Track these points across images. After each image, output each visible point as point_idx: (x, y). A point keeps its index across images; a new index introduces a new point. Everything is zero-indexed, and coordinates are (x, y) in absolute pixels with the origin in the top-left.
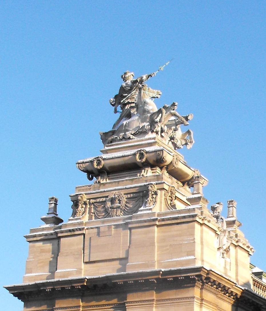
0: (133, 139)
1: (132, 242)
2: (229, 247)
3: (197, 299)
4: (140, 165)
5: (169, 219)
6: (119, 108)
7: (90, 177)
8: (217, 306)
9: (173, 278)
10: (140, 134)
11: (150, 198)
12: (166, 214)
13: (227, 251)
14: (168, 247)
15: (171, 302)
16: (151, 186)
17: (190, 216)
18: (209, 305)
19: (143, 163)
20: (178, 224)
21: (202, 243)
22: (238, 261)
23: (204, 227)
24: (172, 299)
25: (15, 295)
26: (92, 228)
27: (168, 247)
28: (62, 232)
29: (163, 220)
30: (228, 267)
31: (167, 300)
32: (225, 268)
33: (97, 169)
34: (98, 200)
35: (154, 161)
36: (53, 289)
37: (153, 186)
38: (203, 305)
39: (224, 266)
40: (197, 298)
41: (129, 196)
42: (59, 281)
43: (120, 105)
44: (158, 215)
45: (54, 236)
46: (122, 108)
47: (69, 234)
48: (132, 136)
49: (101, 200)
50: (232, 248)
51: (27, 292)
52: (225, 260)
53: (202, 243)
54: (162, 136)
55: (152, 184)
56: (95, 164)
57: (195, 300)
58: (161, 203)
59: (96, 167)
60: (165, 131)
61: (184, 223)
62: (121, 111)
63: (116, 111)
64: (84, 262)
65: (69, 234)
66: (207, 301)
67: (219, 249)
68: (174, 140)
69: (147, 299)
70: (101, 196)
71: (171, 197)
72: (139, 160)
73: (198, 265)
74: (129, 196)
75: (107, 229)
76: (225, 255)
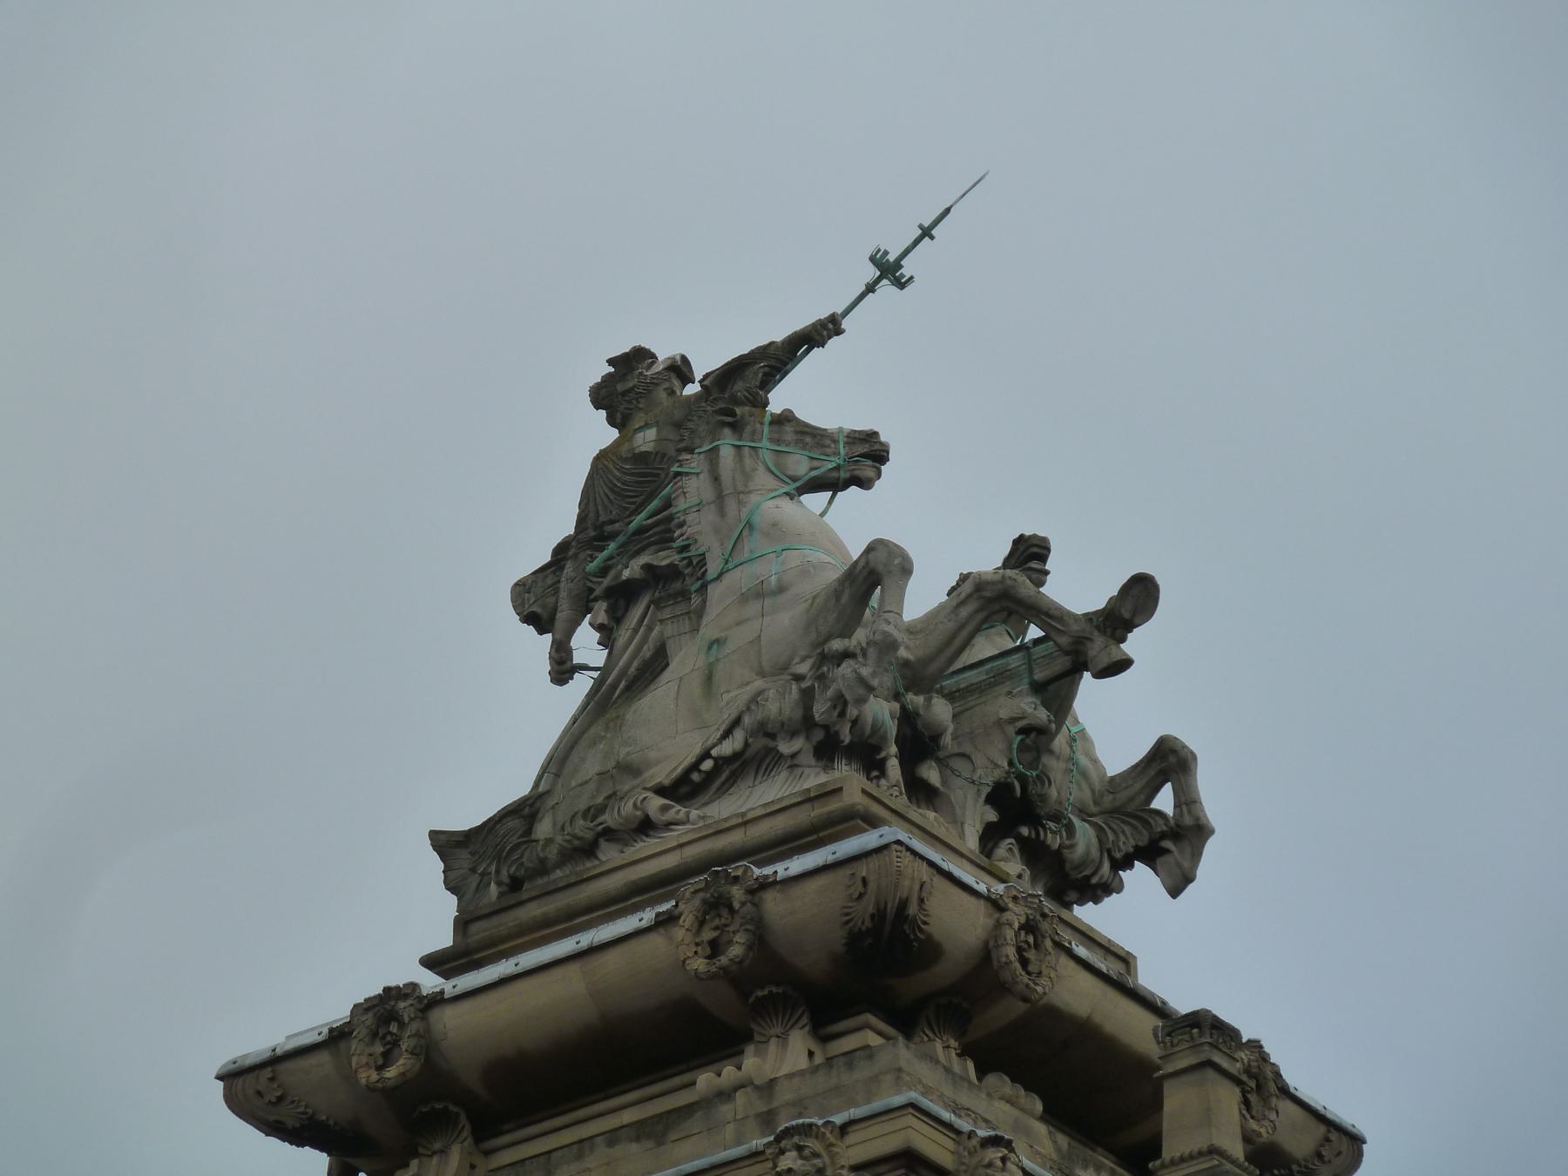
0: (668, 825)
6: (587, 645)
16: (799, 1148)
19: (738, 979)
46: (607, 641)
48: (657, 802)
54: (920, 791)
55: (807, 1130)
56: (360, 1052)
59: (374, 1076)
63: (563, 670)
68: (1035, 821)
72: (699, 964)
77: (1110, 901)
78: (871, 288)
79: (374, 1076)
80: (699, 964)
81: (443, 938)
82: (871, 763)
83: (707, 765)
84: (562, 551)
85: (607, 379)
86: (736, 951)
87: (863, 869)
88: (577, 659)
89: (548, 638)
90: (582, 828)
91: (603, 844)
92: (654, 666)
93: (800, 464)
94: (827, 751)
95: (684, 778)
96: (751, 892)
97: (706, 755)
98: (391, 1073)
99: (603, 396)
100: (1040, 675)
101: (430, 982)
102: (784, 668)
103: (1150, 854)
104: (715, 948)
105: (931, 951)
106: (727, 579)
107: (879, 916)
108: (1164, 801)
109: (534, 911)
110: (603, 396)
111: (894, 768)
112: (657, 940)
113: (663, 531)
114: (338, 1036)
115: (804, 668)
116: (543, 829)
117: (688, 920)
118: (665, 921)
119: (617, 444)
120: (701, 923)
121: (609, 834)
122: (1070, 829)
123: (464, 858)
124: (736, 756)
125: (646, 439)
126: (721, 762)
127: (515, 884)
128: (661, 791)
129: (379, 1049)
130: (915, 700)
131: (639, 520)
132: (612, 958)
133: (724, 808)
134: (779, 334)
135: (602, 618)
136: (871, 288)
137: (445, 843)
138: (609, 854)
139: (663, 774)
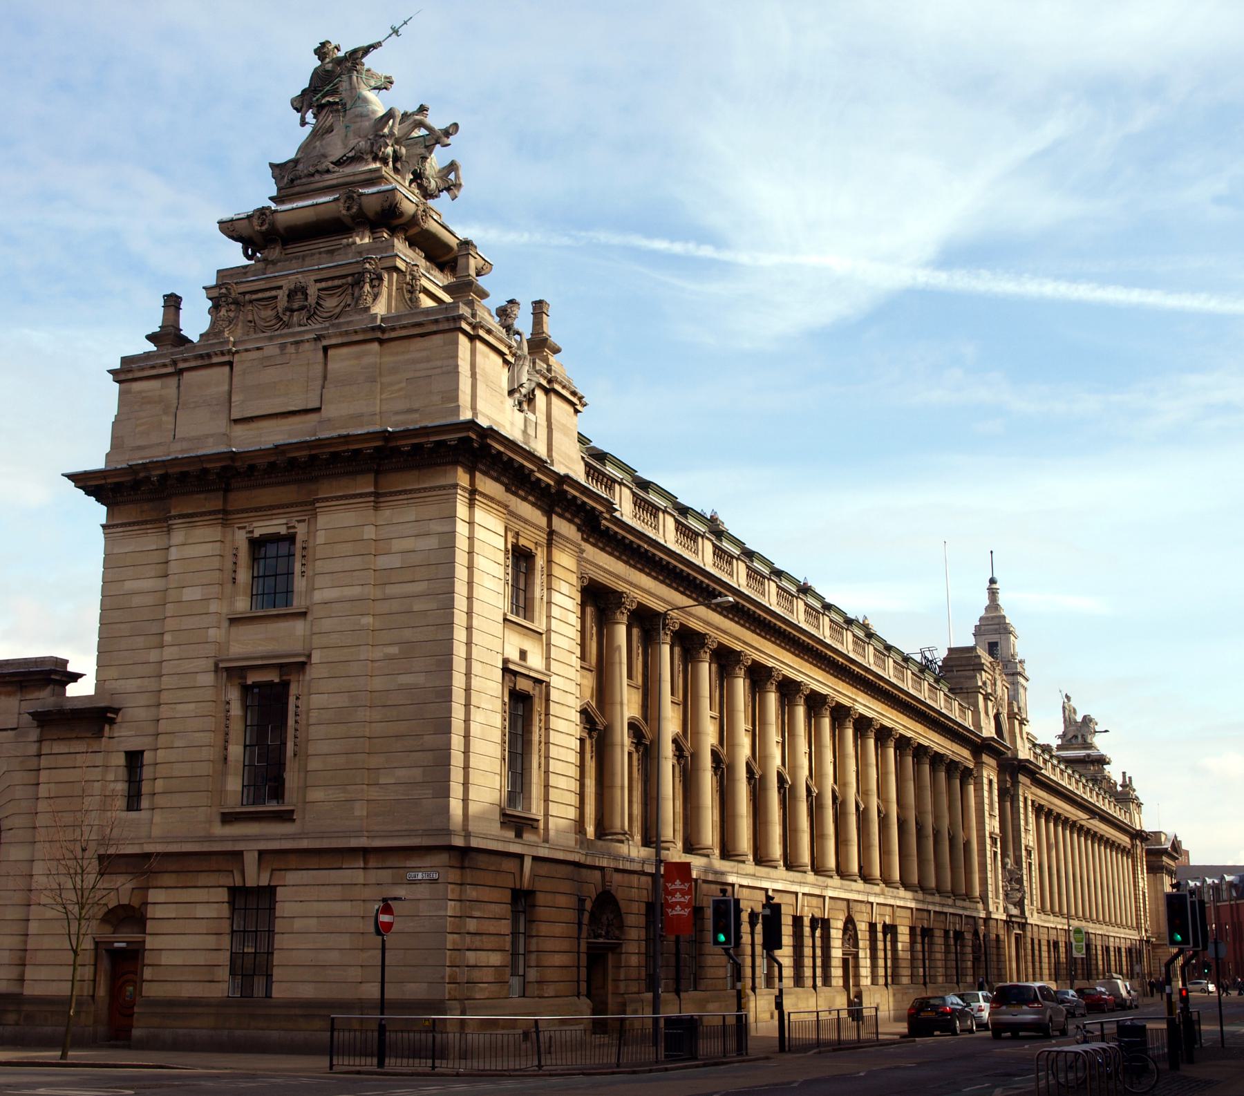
0: (334, 172)
1: (329, 376)
2: (533, 390)
3: (464, 489)
4: (348, 221)
5: (404, 327)
6: (310, 116)
7: (250, 252)
8: (506, 507)
9: (413, 445)
10: (350, 163)
11: (367, 287)
12: (398, 317)
13: (530, 399)
14: (403, 385)
15: (409, 496)
16: (369, 263)
17: (447, 319)
18: (490, 504)
19: (353, 217)
20: (422, 335)
21: (474, 375)
22: (553, 421)
23: (479, 345)
24: (411, 491)
25: (89, 492)
26: (247, 350)
27: (403, 385)
28: (185, 360)
29: (393, 329)
30: (531, 431)
31: (400, 493)
32: (525, 432)
33: (261, 233)
34: (260, 295)
35: (377, 213)
36: (164, 478)
37: (373, 262)
38: (477, 502)
39: (523, 428)
40: (464, 488)
41: (324, 285)
42: (176, 459)
43: (311, 110)
44: (383, 320)
45: (170, 370)
46: (316, 116)
47: (199, 363)
49: (268, 294)
50: (539, 395)
51: (111, 484)
52: (525, 417)
53: (474, 375)
54: (396, 170)
55: (371, 258)
56: (255, 222)
57: (459, 491)
58: (390, 295)
59: (259, 228)
60: (404, 158)
61: (435, 333)
62: (314, 121)
63: (303, 123)
64: (230, 420)
65: (199, 363)
66: (482, 494)
68: (421, 179)
69: (358, 492)
70: (268, 286)
71: (412, 286)
72: (344, 212)
73: (466, 415)
74: (324, 285)
75: (277, 351)
76: (525, 406)
77: (436, 200)
78: (390, 36)
79: (259, 228)
80: (344, 212)
81: (274, 193)
82: (386, 163)
83: (345, 158)
84: (304, 92)
85: (319, 48)
86: (354, 210)
87: (387, 194)
88: (307, 120)
89: (300, 114)
90: (312, 170)
91: (316, 174)
92: (330, 130)
93: (373, 83)
95: (339, 161)
96: (359, 196)
97: (345, 155)
98: (264, 228)
99: (317, 52)
100: (427, 144)
101: (273, 206)
102: (366, 136)
103: (448, 189)
104: (349, 209)
105: (402, 214)
106: (352, 111)
107: (390, 206)
108: (452, 176)
109: (297, 189)
110: (317, 52)
111: (391, 164)
112: (333, 205)
114: (249, 217)
115: (371, 137)
116: (300, 167)
117: (342, 201)
118: (336, 200)
119: (320, 66)
120: (345, 202)
121: (317, 171)
122: (430, 182)
123: (277, 171)
124: (352, 157)
125: (329, 67)
126: (348, 158)
127: (292, 181)
128: (332, 163)
129: (260, 221)
130: (397, 147)
131: (328, 88)
132: (322, 207)
133: (349, 170)
134: (366, 44)
135: (315, 112)
136: (390, 36)
137: (272, 166)
138: (317, 177)
139: (334, 159)
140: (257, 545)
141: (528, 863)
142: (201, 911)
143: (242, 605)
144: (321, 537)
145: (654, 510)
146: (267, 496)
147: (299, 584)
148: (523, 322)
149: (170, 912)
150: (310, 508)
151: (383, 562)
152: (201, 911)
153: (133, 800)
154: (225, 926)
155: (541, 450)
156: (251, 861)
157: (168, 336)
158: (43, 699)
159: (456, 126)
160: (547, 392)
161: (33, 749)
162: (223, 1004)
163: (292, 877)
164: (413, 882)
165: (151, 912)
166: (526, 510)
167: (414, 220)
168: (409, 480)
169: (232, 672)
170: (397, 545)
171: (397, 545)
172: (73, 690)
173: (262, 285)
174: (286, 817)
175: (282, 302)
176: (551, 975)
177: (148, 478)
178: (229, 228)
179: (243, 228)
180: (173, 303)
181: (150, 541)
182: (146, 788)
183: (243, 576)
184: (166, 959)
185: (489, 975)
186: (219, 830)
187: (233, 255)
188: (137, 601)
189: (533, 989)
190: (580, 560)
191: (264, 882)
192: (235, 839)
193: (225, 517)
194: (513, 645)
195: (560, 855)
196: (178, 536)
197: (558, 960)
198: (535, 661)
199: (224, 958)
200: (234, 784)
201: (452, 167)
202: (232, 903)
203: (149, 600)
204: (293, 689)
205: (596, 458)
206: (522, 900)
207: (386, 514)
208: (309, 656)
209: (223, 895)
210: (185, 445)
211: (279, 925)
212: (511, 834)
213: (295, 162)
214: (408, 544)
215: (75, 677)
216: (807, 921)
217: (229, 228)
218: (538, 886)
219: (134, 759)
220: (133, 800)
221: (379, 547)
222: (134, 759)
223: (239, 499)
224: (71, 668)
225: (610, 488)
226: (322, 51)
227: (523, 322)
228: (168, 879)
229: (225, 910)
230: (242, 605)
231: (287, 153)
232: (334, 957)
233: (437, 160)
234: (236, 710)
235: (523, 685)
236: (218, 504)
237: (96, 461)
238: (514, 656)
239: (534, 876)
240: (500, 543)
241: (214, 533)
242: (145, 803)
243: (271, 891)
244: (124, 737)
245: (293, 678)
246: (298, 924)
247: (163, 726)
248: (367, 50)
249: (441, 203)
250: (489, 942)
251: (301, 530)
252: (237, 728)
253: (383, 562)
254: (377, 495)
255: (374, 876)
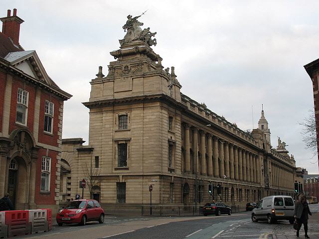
6: (126, 30)
13: (172, 87)
56: (117, 53)
63: (125, 31)
67: (168, 86)
94: (140, 40)
113: (132, 25)
140: (119, 116)
141: (173, 178)
142: (111, 187)
143: (117, 128)
144: (133, 116)
145: (194, 106)
146: (122, 107)
147: (128, 124)
148: (170, 72)
149: (105, 187)
150: (130, 110)
151: (145, 120)
152: (111, 187)
153: (97, 166)
154: (116, 189)
155: (173, 97)
156: (121, 177)
157: (100, 75)
158: (78, 146)
159: (156, 33)
160: (175, 85)
161: (77, 156)
162: (116, 204)
163: (129, 180)
164: (152, 181)
165: (101, 187)
166: (171, 109)
167: (148, 52)
168: (150, 105)
169: (116, 141)
170: (148, 117)
171: (148, 117)
172: (83, 144)
173: (119, 65)
174: (127, 169)
175: (123, 69)
176: (177, 199)
177: (98, 104)
178: (112, 54)
179: (115, 54)
180: (101, 68)
181: (99, 116)
182: (99, 163)
183: (117, 123)
184: (105, 196)
185: (167, 199)
186: (114, 171)
187: (113, 59)
188: (96, 127)
189: (174, 202)
190: (181, 118)
191: (123, 181)
192: (117, 173)
193: (113, 111)
194: (169, 136)
195: (178, 176)
196: (104, 115)
197: (178, 196)
198: (173, 139)
199: (116, 196)
200: (117, 163)
201: (155, 40)
202: (117, 185)
203: (99, 127)
204: (128, 145)
205: (183, 96)
206: (172, 184)
207: (145, 111)
208: (131, 138)
209: (116, 184)
210: (105, 97)
211: (127, 189)
212: (170, 172)
213: (124, 40)
214: (150, 117)
215: (84, 142)
216: (224, 188)
217: (112, 54)
218: (175, 182)
219: (97, 158)
220: (97, 166)
221: (144, 118)
222: (97, 158)
223: (116, 108)
224: (83, 140)
225: (186, 103)
226: (129, 17)
227: (170, 72)
228: (104, 181)
229: (116, 187)
230: (117, 128)
231: (122, 38)
232: (137, 195)
233: (152, 38)
234: (117, 149)
235: (171, 143)
236: (112, 109)
237: (88, 101)
238: (170, 138)
239: (174, 180)
240: (167, 116)
241: (111, 114)
242: (99, 166)
243: (125, 183)
244: (95, 154)
245: (128, 142)
246: (130, 189)
247: (103, 152)
248: (138, 17)
249: (152, 47)
250: (166, 193)
251: (129, 114)
252: (117, 152)
253: (145, 120)
254: (144, 107)
255: (145, 180)
